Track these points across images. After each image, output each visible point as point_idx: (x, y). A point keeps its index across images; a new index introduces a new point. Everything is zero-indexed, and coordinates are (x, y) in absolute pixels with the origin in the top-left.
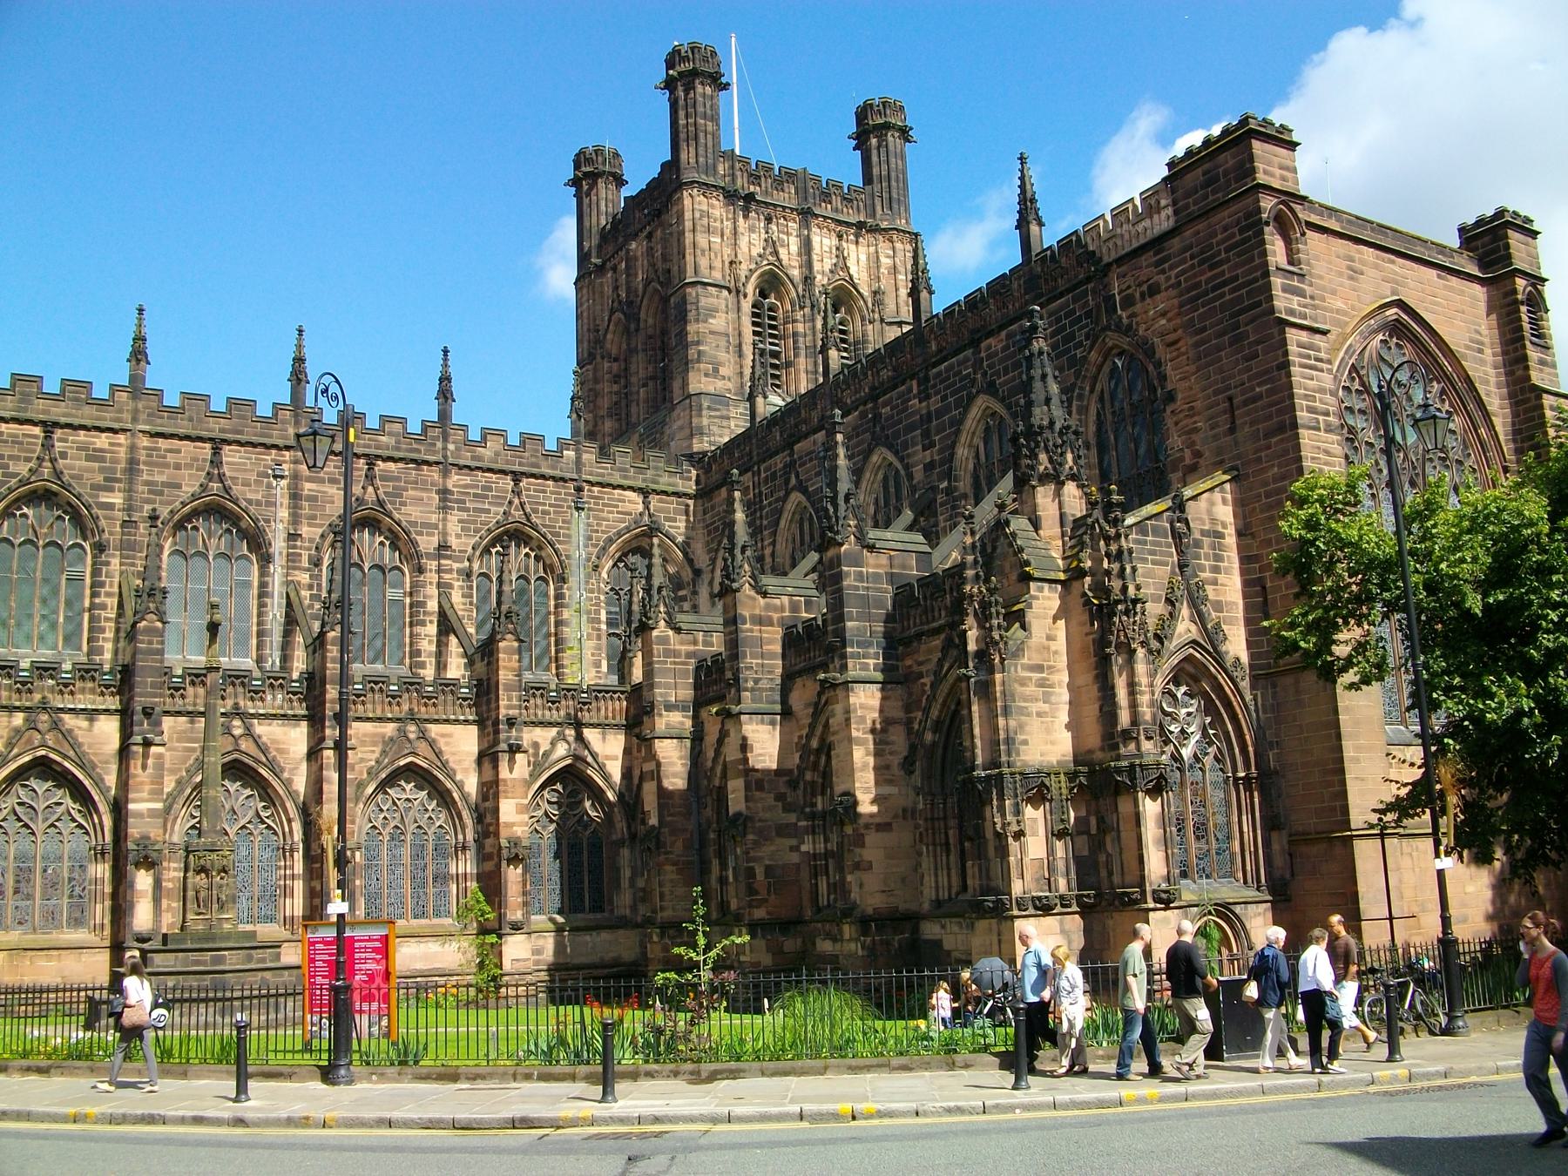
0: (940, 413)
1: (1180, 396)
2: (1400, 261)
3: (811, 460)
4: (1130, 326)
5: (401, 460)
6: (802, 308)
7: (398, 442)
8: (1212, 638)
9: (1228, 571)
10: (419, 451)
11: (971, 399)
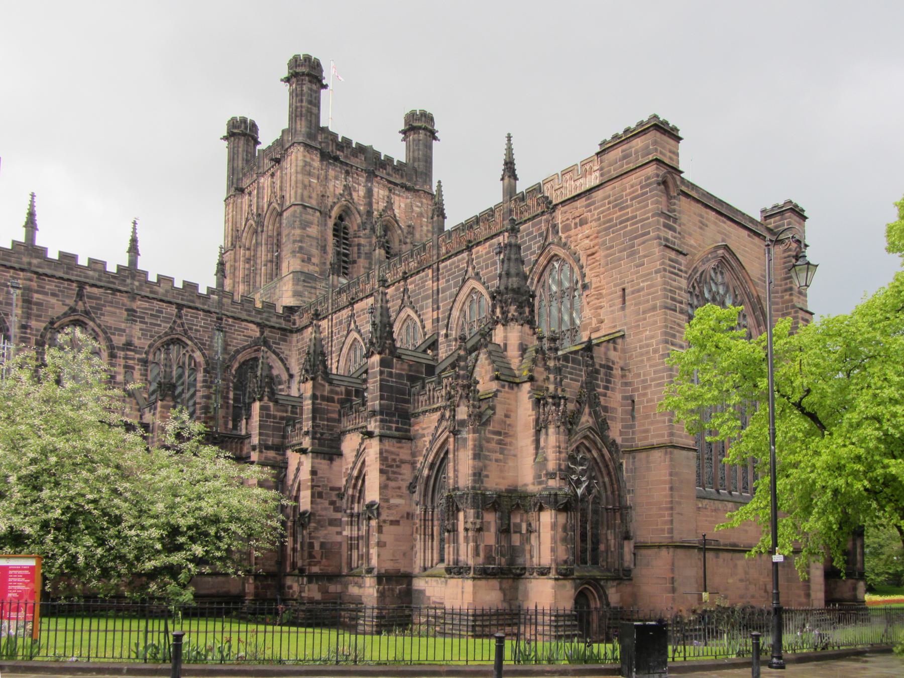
1: (593, 286)
2: (729, 223)
4: (565, 244)
5: (101, 287)
7: (100, 276)
8: (602, 427)
9: (613, 390)
10: (114, 283)
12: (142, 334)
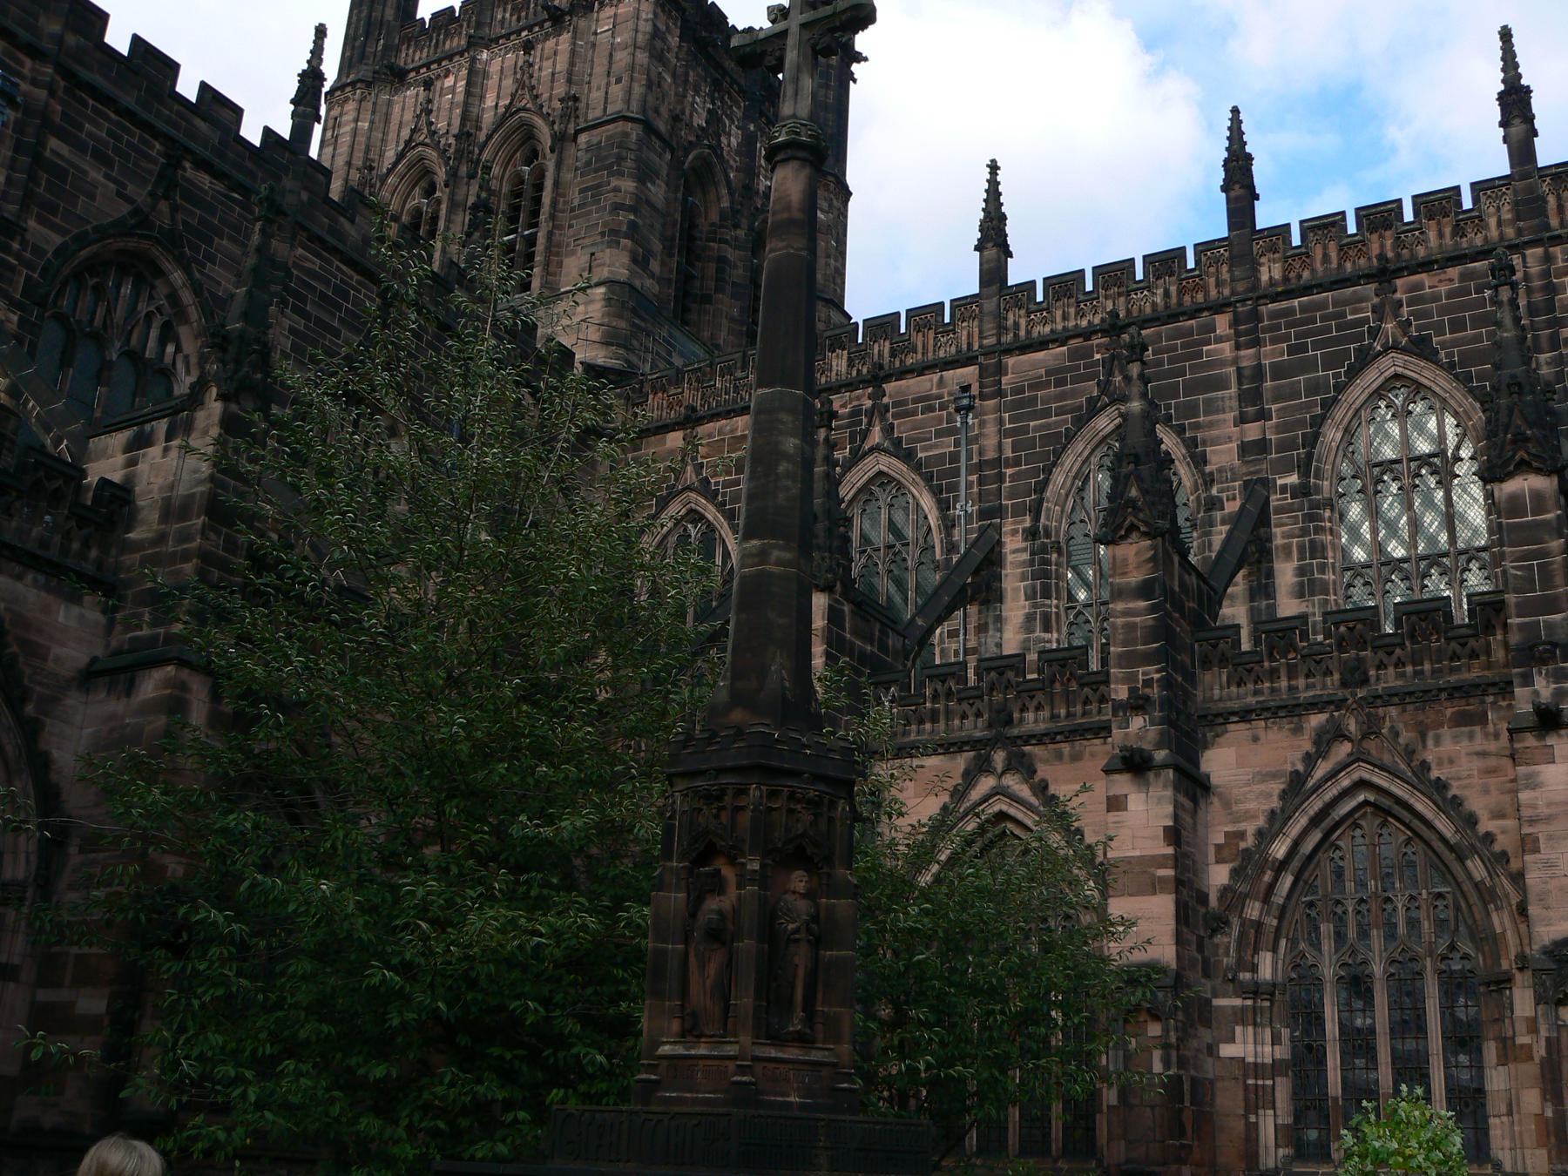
0: (1279, 371)
3: (931, 409)
5: (217, 175)
6: (736, 226)
11: (1365, 359)
12: (294, 347)
